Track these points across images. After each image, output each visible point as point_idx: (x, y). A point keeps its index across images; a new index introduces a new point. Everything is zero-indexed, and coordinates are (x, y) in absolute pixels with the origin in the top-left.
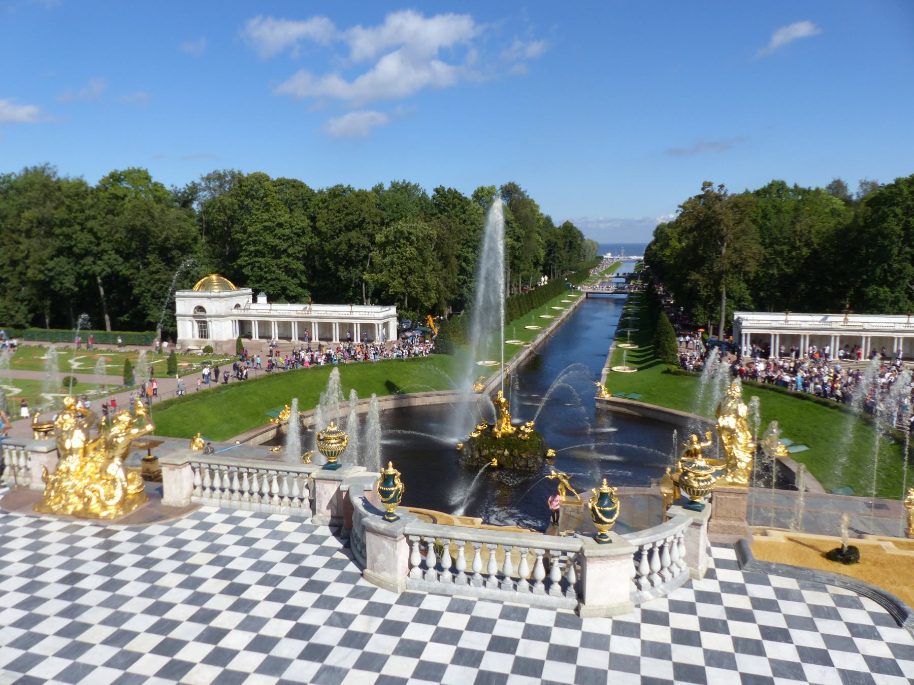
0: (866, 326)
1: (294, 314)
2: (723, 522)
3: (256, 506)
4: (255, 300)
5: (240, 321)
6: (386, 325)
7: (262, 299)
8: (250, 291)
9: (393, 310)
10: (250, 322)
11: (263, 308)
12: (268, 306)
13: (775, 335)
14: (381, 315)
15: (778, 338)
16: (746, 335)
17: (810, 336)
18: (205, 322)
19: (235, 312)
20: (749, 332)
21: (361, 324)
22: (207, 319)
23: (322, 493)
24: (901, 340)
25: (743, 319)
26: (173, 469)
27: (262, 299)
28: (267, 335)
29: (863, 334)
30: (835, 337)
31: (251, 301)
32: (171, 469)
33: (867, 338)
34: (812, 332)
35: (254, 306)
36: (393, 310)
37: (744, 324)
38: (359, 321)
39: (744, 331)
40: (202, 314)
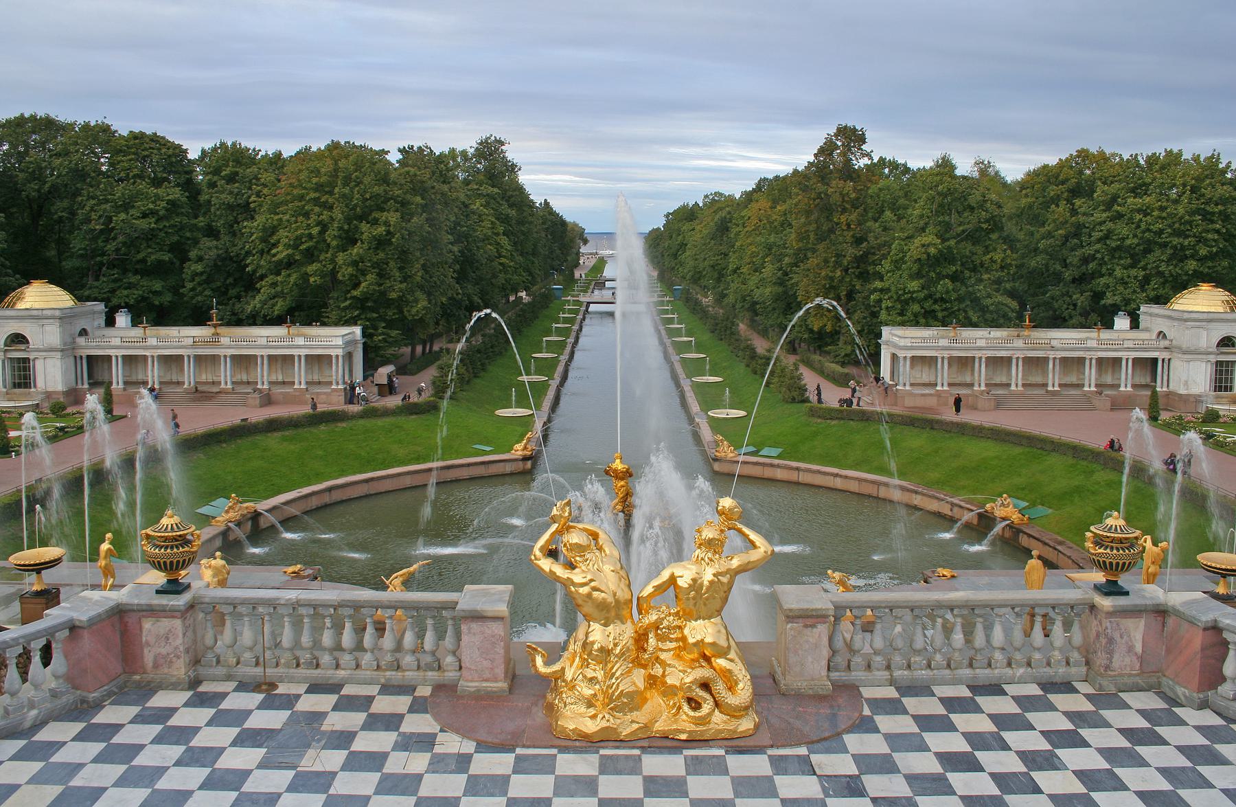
0: (1054, 343)
3: (967, 672)
4: (110, 322)
5: (88, 357)
7: (122, 319)
8: (100, 307)
11: (124, 337)
12: (138, 332)
15: (946, 362)
19: (81, 341)
20: (910, 354)
23: (1117, 636)
24: (1094, 362)
26: (813, 626)
27: (122, 319)
28: (134, 379)
29: (1051, 355)
32: (806, 626)
33: (1054, 359)
34: (990, 354)
35: (110, 332)
36: (357, 330)
38: (303, 352)
39: (901, 354)
40: (23, 347)
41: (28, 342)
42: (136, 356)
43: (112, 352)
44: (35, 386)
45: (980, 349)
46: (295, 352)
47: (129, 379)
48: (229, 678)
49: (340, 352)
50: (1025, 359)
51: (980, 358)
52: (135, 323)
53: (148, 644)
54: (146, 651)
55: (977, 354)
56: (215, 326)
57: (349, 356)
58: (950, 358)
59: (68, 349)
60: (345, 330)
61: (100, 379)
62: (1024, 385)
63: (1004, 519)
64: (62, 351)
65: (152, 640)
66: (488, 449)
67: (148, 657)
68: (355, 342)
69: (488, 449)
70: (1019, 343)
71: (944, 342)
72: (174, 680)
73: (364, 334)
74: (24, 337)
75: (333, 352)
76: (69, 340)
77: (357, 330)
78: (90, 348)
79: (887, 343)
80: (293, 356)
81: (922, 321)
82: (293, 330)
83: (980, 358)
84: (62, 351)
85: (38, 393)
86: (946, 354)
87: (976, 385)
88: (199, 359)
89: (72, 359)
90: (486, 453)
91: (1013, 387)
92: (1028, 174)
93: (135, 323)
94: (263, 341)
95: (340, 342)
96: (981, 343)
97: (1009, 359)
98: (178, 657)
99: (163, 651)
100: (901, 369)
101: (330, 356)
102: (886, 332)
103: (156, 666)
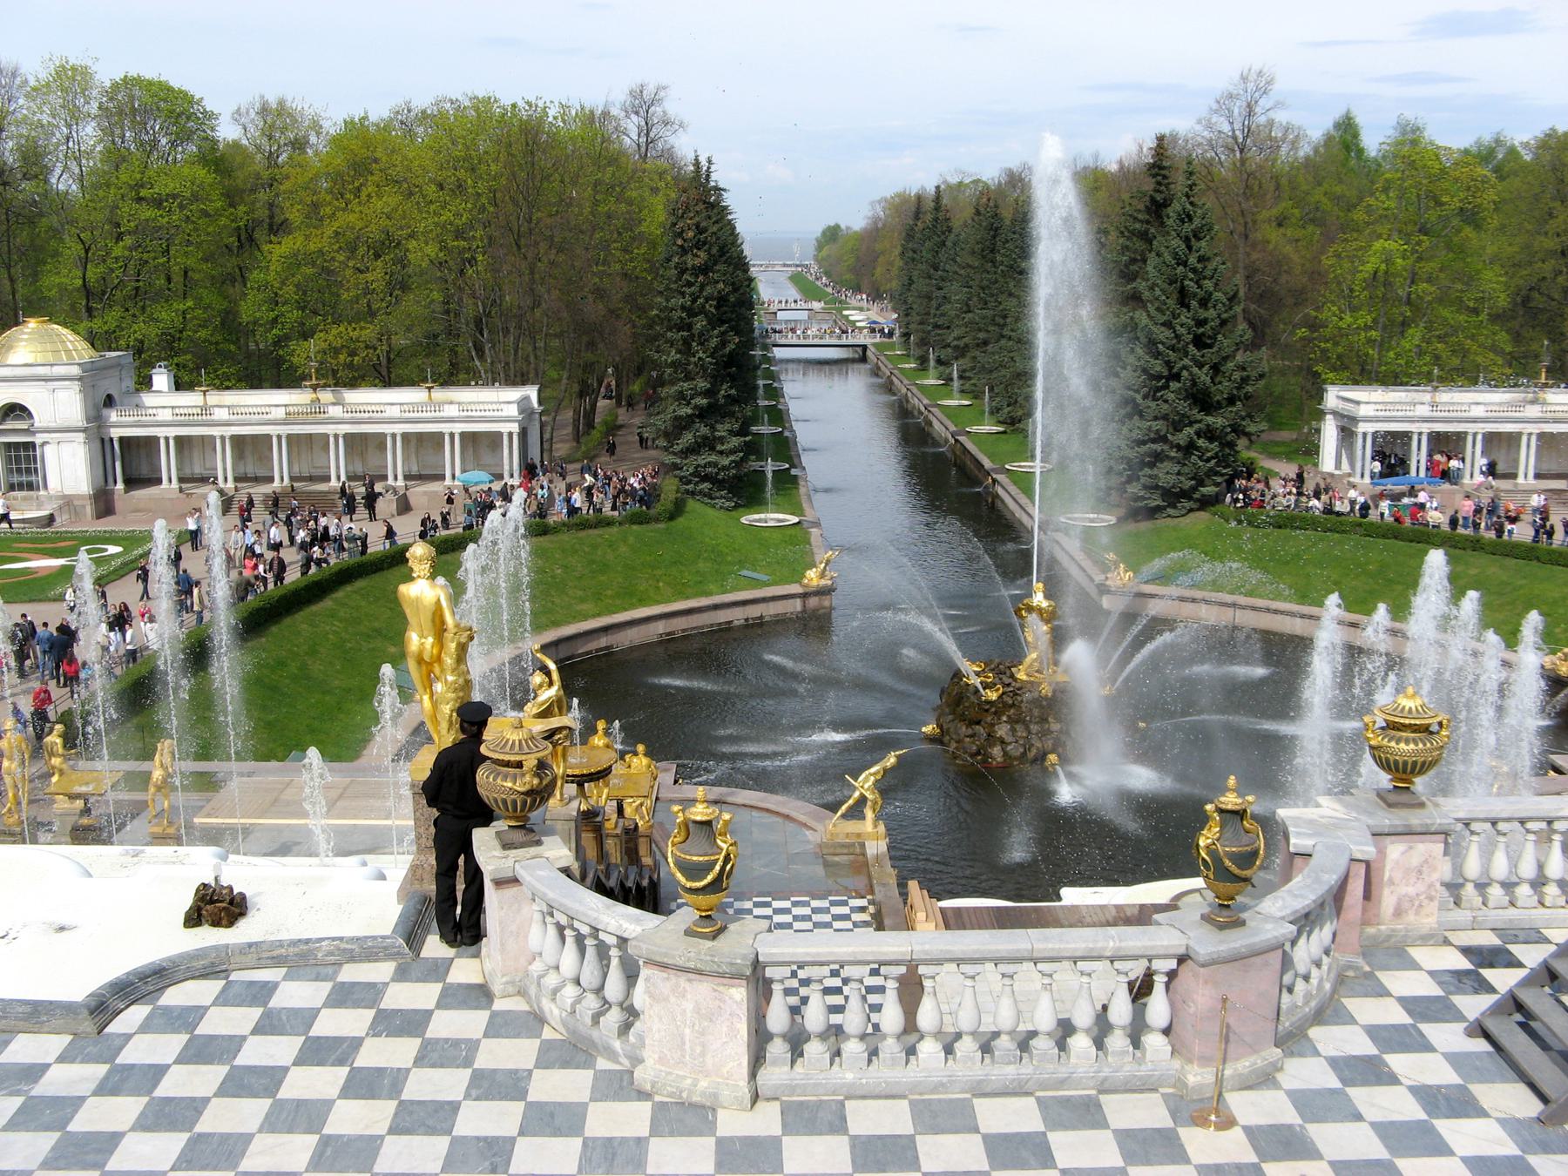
1: (279, 413)
4: (145, 383)
5: (121, 439)
7: (161, 379)
10: (157, 439)
11: (164, 407)
12: (191, 399)
16: (1365, 435)
18: (33, 445)
20: (1370, 428)
21: (463, 434)
22: (38, 439)
25: (1358, 403)
27: (161, 379)
30: (1530, 434)
31: (129, 383)
36: (532, 392)
38: (458, 428)
39: (1362, 428)
41: (30, 415)
42: (189, 438)
43: (160, 432)
44: (46, 487)
45: (1474, 421)
47: (187, 472)
48: (1474, 926)
49: (515, 427)
50: (1541, 436)
51: (1475, 435)
52: (179, 386)
53: (1391, 882)
54: (1386, 892)
56: (315, 388)
57: (524, 434)
59: (96, 430)
60: (514, 394)
61: (135, 474)
62: (1538, 476)
64: (85, 430)
65: (1398, 876)
66: (765, 578)
67: (1388, 900)
70: (1533, 411)
71: (1422, 411)
72: (1424, 931)
74: (23, 409)
75: (505, 428)
76: (92, 413)
77: (532, 392)
78: (121, 424)
79: (1335, 413)
80: (439, 436)
82: (439, 394)
83: (1475, 435)
84: (85, 430)
85: (50, 498)
86: (1426, 428)
88: (297, 443)
89: (98, 444)
91: (1520, 480)
92: (1484, 155)
93: (179, 386)
94: (394, 412)
95: (513, 411)
96: (1478, 412)
97: (1520, 434)
98: (1431, 899)
99: (1411, 890)
100: (1359, 453)
101: (500, 434)
102: (1333, 397)
103: (1398, 913)
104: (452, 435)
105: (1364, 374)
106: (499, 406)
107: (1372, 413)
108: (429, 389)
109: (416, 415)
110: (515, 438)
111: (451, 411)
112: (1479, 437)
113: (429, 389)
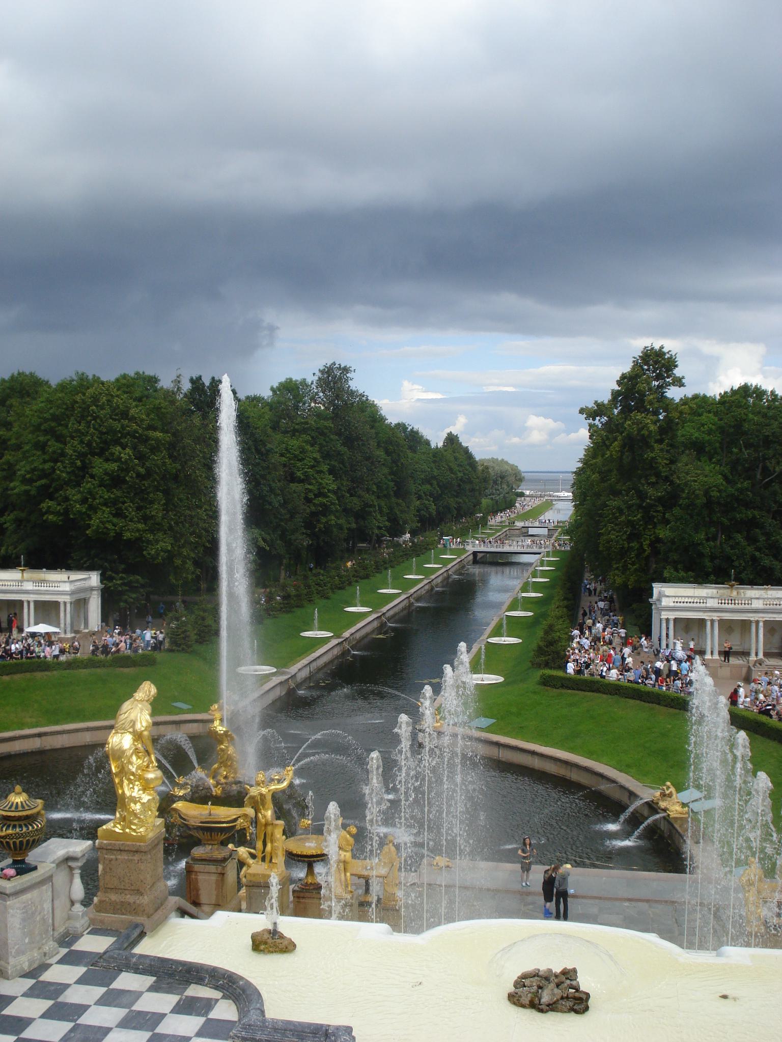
2: (114, 897)
6: (80, 604)
9: (94, 579)
13: (712, 621)
14: (67, 587)
15: (716, 625)
16: (667, 620)
17: (765, 622)
20: (672, 616)
21: (36, 602)
37: (665, 602)
46: (23, 597)
49: (67, 599)
55: (752, 617)
57: (80, 604)
58: (721, 621)
63: (665, 810)
68: (92, 589)
69: (185, 706)
73: (103, 578)
75: (61, 599)
81: (712, 577)
82: (29, 574)
83: (757, 622)
86: (716, 616)
87: (753, 654)
90: (181, 711)
101: (57, 604)
102: (657, 588)
104: (29, 602)
105: (697, 573)
106: (61, 584)
107: (672, 604)
108: (23, 571)
109: (16, 588)
110: (68, 606)
111: (29, 586)
112: (761, 624)
113: (23, 571)
